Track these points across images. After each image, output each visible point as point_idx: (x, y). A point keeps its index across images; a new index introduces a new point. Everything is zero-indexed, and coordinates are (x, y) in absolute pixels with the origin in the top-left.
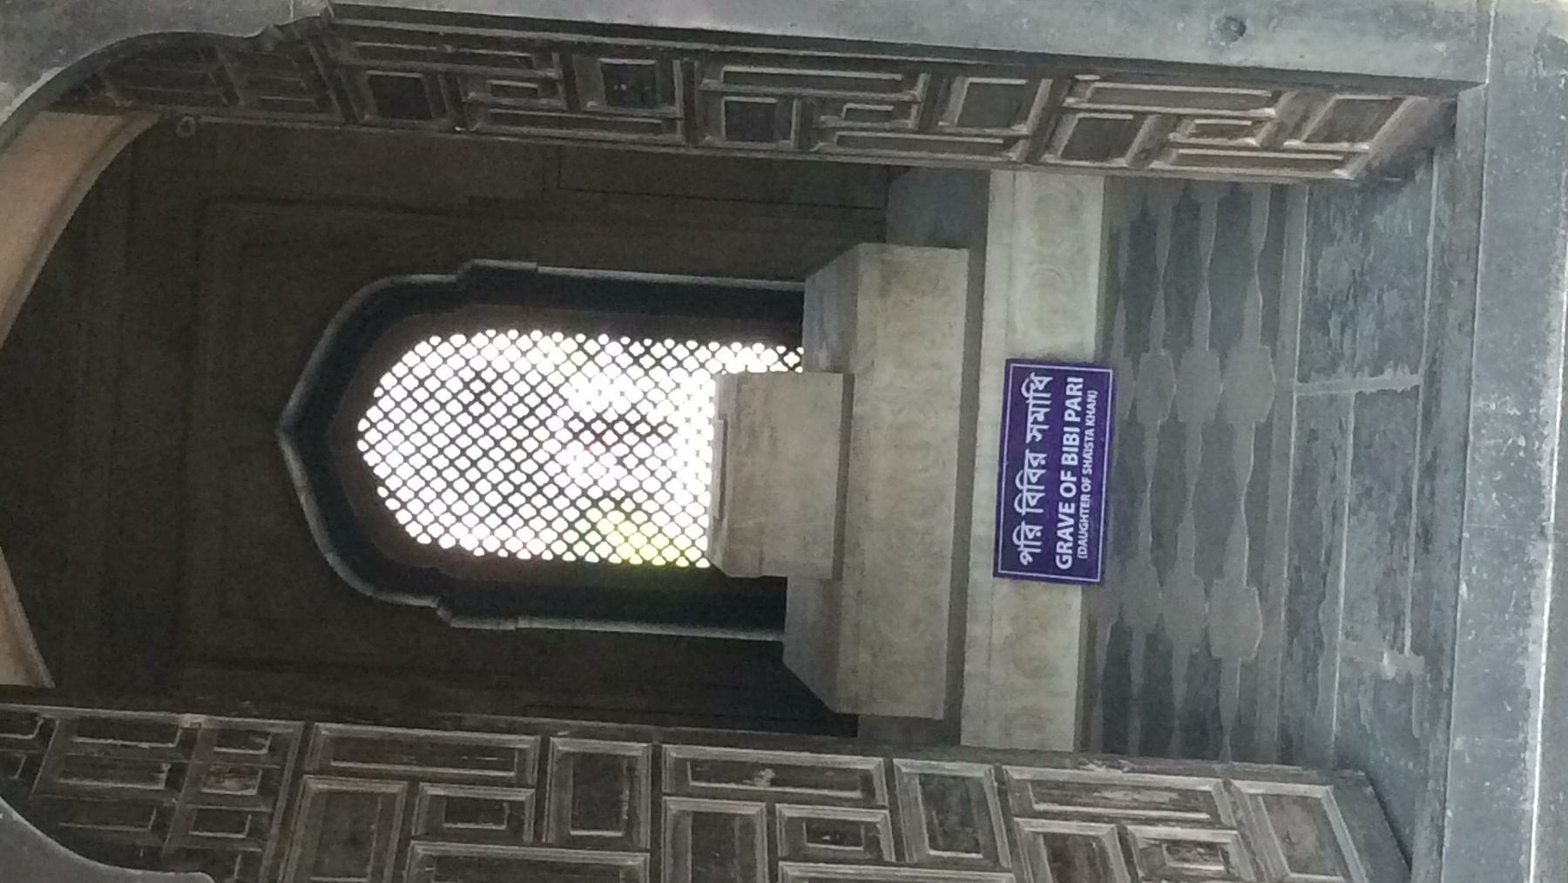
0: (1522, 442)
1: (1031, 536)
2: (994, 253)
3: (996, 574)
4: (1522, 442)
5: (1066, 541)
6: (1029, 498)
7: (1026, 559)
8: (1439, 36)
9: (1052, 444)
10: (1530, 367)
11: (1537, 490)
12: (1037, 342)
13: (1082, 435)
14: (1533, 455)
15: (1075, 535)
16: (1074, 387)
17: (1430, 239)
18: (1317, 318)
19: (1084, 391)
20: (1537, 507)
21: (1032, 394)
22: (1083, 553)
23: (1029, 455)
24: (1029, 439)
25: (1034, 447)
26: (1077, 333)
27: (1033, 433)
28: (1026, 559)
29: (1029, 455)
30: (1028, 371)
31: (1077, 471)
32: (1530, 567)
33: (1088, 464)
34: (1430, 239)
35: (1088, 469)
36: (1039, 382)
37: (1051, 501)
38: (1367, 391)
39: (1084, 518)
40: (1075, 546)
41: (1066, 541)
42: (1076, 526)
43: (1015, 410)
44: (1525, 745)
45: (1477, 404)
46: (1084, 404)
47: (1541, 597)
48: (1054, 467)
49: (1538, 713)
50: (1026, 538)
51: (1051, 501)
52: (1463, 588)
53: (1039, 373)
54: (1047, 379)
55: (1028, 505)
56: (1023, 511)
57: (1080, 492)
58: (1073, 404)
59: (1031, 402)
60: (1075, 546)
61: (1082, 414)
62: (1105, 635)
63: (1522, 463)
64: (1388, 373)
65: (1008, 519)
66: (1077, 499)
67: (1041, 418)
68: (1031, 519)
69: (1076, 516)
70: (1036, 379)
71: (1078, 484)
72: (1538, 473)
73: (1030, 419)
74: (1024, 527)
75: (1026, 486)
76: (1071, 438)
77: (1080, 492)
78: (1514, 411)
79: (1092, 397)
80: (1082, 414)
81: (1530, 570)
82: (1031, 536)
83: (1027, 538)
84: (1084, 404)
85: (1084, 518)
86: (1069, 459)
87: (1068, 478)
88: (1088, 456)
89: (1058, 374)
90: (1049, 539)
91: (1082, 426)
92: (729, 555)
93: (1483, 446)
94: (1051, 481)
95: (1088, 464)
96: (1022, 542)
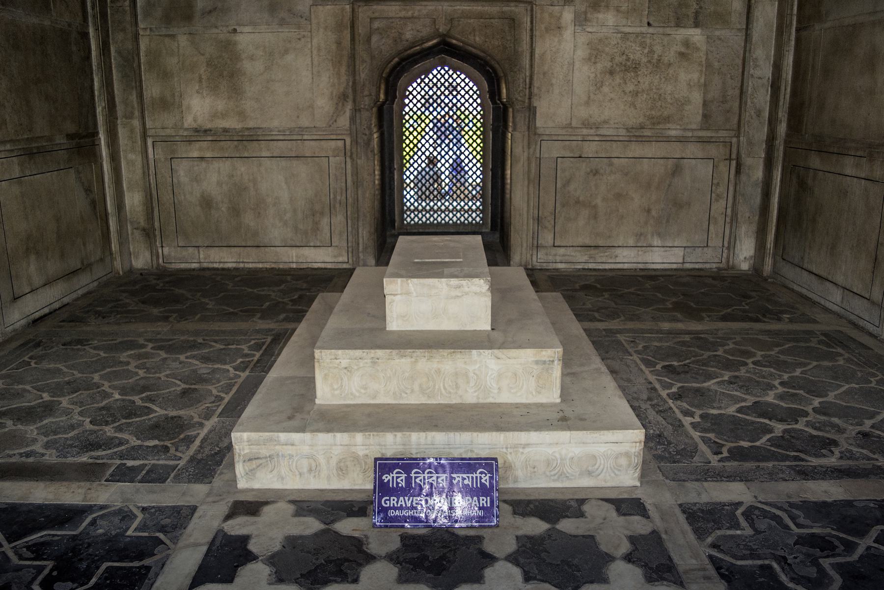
1: (399, 480)
3: (376, 459)
5: (397, 503)
7: (386, 478)
15: (401, 508)
21: (478, 475)
22: (392, 513)
24: (453, 475)
28: (386, 478)
30: (491, 472)
36: (485, 479)
40: (395, 508)
41: (397, 503)
50: (397, 477)
53: (491, 478)
54: (488, 484)
55: (416, 478)
56: (413, 475)
59: (474, 476)
60: (395, 508)
67: (466, 482)
68: (408, 480)
70: (487, 477)
73: (465, 476)
74: (404, 476)
75: (426, 475)
82: (399, 480)
83: (395, 478)
96: (395, 475)
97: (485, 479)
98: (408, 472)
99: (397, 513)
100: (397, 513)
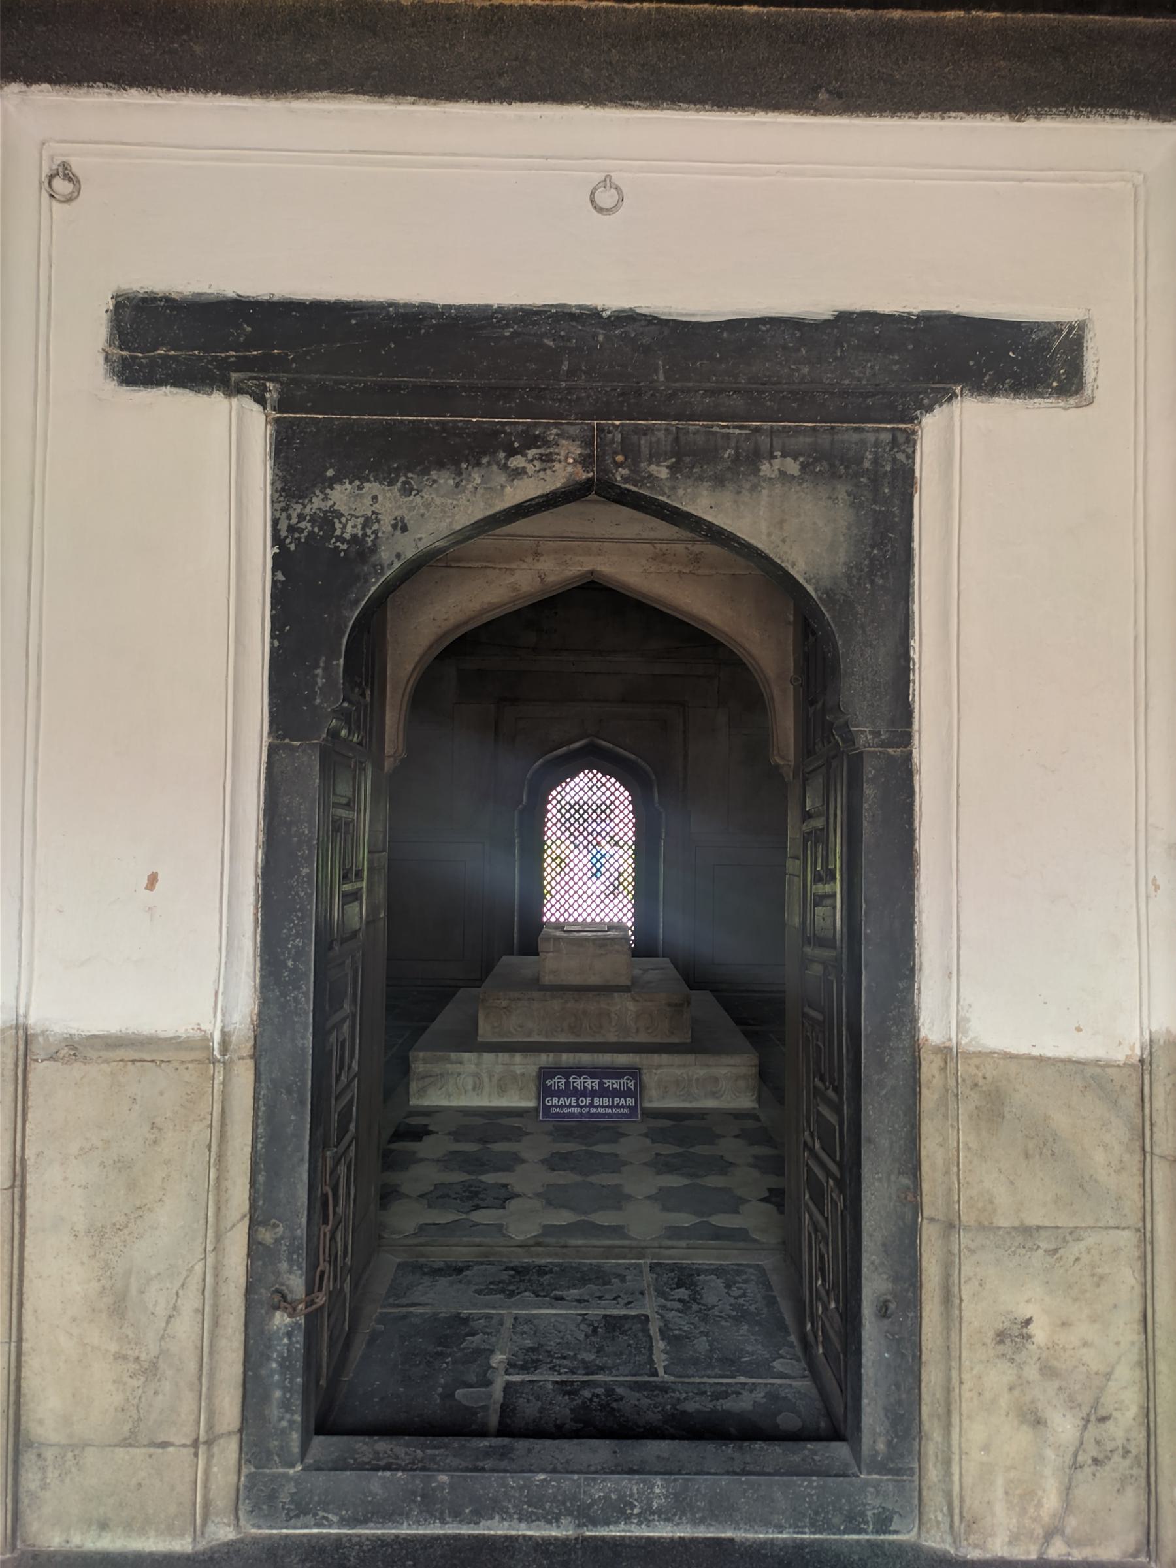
0: (636, 1511)
2: (691, 1058)
4: (636, 1511)
6: (577, 1083)
7: (549, 1083)
8: (889, 1444)
9: (603, 1092)
10: (683, 1513)
11: (607, 1523)
12: (650, 1079)
13: (608, 1107)
14: (628, 1519)
15: (561, 1106)
16: (630, 1102)
17: (742, 1379)
18: (685, 1277)
19: (629, 1107)
20: (594, 1523)
22: (553, 1110)
23: (597, 1081)
25: (601, 1084)
26: (655, 1100)
27: (608, 1083)
29: (597, 1081)
31: (591, 1105)
32: (557, 1521)
33: (595, 1110)
34: (742, 1379)
35: (593, 1111)
36: (631, 1084)
37: (579, 1093)
38: (650, 1326)
39: (569, 1110)
40: (556, 1106)
42: (566, 1106)
43: (617, 1073)
44: (443, 1522)
45: (658, 1481)
46: (622, 1107)
47: (539, 1528)
48: (593, 1094)
49: (466, 1530)
51: (579, 1093)
52: (542, 1477)
56: (571, 1080)
57: (582, 1107)
58: (622, 1102)
60: (556, 1106)
61: (618, 1106)
62: (516, 1122)
63: (622, 1512)
64: (661, 1345)
65: (567, 1073)
66: (578, 1106)
68: (567, 1084)
69: (570, 1106)
71: (585, 1106)
72: (617, 1522)
74: (563, 1081)
76: (606, 1101)
77: (582, 1107)
78: (655, 1505)
79: (626, 1111)
80: (618, 1106)
81: (553, 1519)
83: (558, 1083)
84: (622, 1107)
85: (569, 1110)
86: (596, 1101)
87: (587, 1101)
88: (599, 1110)
89: (637, 1093)
90: (559, 1094)
91: (612, 1106)
92: (548, 939)
93: (632, 1485)
94: (584, 1093)
95: (595, 1110)
97: (631, 1084)
98: (567, 1078)
99: (558, 1110)
100: (558, 1110)
